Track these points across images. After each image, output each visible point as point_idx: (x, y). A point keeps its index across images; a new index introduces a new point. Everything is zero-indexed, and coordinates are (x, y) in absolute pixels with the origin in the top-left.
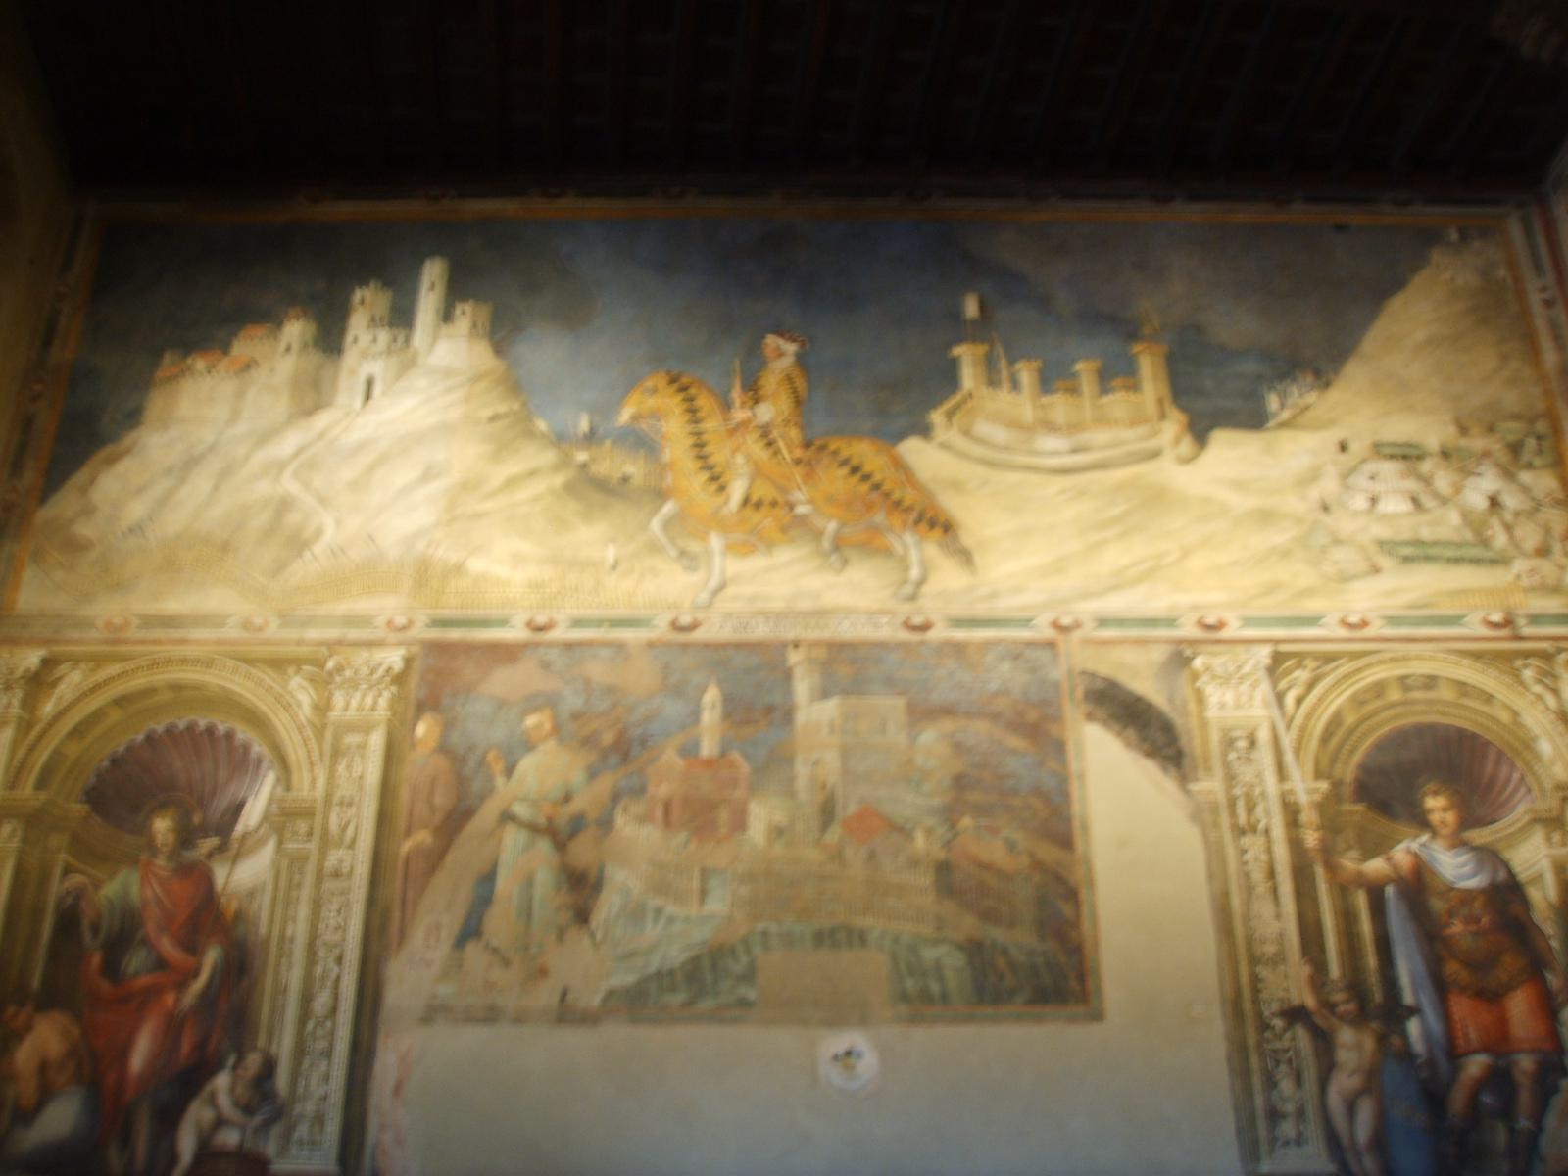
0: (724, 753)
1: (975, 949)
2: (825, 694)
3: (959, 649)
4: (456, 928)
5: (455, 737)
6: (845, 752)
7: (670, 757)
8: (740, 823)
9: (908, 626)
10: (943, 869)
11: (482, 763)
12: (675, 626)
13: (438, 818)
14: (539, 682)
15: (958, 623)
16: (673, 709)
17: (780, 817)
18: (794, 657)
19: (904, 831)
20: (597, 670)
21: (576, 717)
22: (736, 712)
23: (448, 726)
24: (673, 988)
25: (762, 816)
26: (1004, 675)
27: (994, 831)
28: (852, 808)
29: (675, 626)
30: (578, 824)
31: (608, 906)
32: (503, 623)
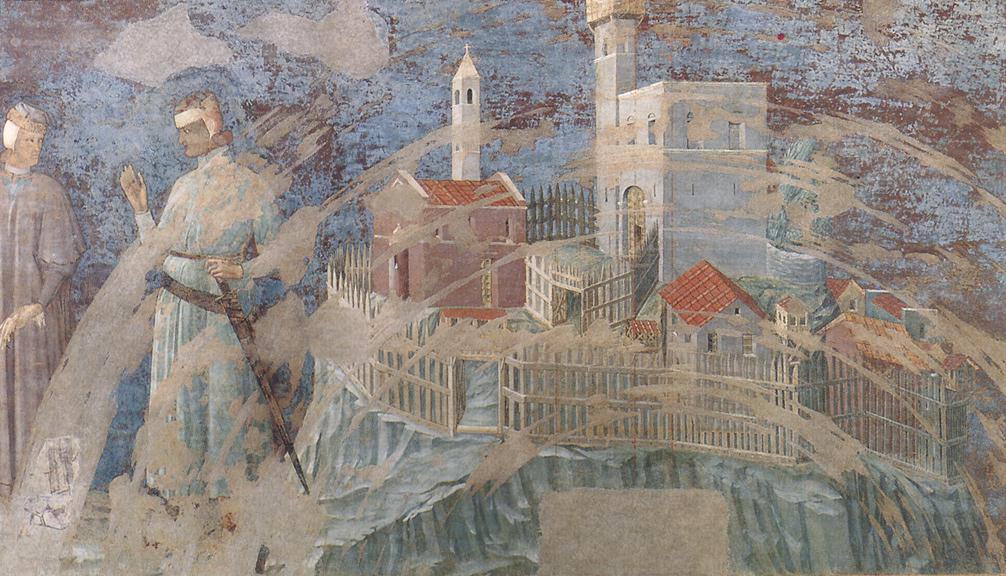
0: (484, 176)
1: (857, 493)
4: (94, 461)
5: (66, 148)
6: (670, 180)
8: (513, 290)
10: (815, 366)
11: (114, 189)
13: (52, 281)
16: (411, 99)
17: (572, 282)
21: (255, 110)
23: (52, 125)
24: (422, 546)
25: (547, 272)
30: (271, 289)
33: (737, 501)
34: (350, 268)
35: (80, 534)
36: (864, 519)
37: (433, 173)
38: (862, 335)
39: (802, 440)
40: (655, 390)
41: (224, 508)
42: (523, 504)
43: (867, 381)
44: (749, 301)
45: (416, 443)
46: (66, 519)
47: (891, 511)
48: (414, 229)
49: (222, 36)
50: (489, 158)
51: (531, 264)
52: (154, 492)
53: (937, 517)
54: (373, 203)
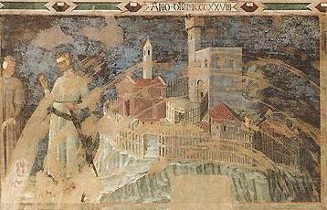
2: (203, 46)
3: (270, 20)
5: (22, 69)
6: (212, 78)
7: (129, 79)
9: (245, 7)
10: (257, 136)
12: (128, 6)
13: (18, 110)
14: (66, 40)
15: (270, 6)
16: (130, 53)
17: (181, 110)
18: (189, 23)
19: (239, 117)
20: (91, 33)
21: (81, 57)
22: (162, 56)
23: (19, 62)
26: (292, 36)
27: (282, 117)
28: (216, 104)
29: (128, 6)
31: (101, 155)
32: (42, 6)
33: (233, 179)
34: (111, 106)
35: (26, 189)
36: (274, 184)
37: (137, 76)
38: (272, 126)
39: (254, 161)
40: (206, 144)
41: (71, 181)
42: (166, 180)
43: (274, 141)
44: (238, 116)
45: (131, 161)
46: (22, 185)
47: (283, 182)
48: (131, 94)
49: (71, 34)
50: (155, 71)
51: (168, 104)
52: (50, 176)
53: (297, 184)
54: (118, 86)
